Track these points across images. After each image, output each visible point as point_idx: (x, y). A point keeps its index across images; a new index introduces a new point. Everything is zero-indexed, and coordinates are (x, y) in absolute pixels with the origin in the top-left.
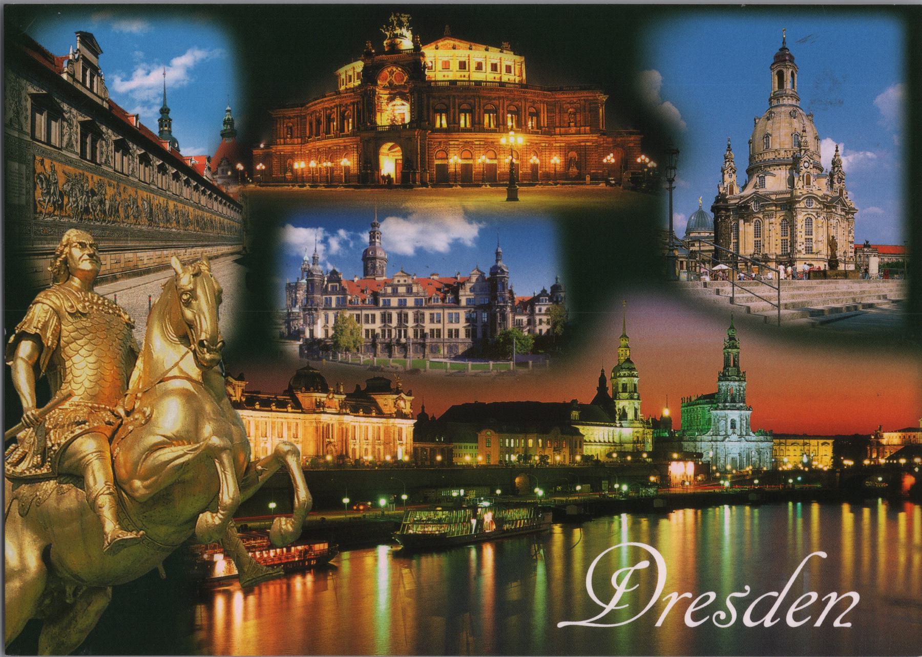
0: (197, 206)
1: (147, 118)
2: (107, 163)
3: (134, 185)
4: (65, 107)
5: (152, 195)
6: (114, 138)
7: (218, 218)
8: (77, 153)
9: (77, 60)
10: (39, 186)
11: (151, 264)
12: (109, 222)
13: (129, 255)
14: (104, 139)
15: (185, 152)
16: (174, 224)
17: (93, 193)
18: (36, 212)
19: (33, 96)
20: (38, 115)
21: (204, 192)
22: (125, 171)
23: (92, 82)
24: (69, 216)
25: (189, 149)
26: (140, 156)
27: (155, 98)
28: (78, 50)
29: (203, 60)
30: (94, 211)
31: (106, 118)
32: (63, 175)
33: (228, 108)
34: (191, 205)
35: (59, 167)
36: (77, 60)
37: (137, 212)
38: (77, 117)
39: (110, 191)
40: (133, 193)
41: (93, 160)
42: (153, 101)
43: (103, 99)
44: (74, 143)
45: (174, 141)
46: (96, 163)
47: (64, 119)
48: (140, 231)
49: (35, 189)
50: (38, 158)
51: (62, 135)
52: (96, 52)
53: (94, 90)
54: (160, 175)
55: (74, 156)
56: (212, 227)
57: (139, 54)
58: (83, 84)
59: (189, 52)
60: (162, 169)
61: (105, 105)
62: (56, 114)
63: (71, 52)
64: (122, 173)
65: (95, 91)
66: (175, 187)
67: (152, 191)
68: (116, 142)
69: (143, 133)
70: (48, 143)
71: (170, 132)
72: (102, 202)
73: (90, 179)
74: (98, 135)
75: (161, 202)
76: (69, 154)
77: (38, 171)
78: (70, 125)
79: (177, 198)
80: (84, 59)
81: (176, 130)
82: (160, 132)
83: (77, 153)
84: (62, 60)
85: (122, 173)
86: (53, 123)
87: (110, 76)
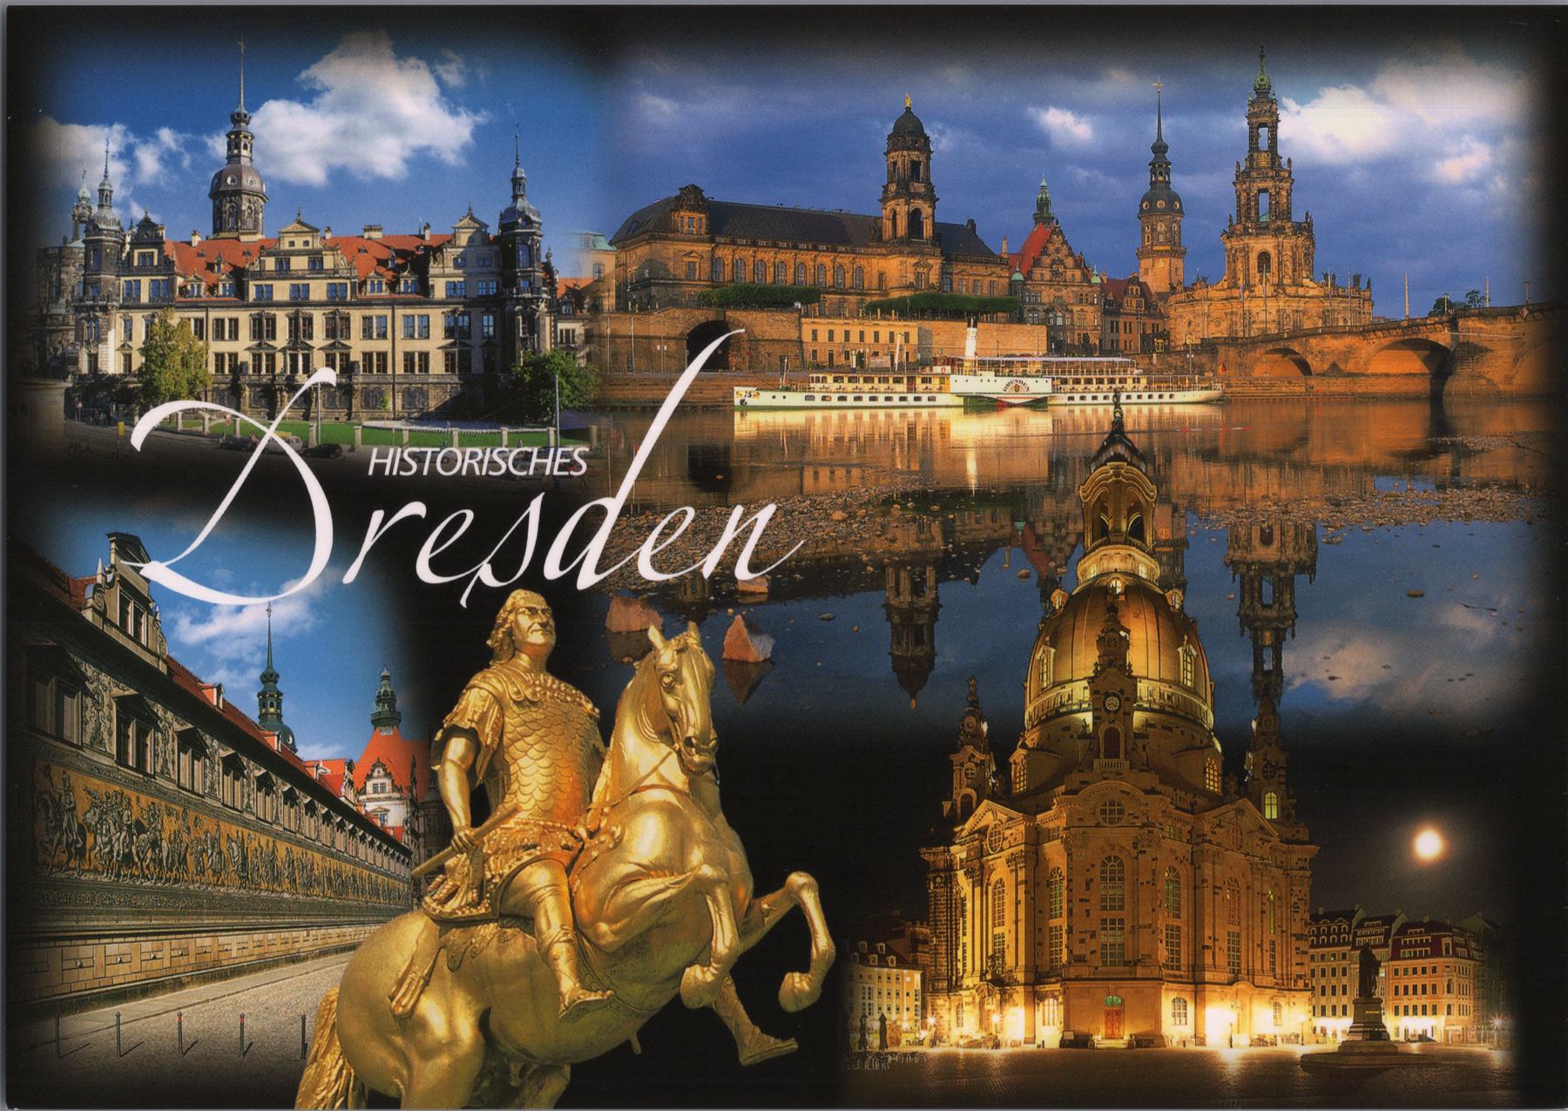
0: (328, 852)
1: (236, 689)
3: (213, 812)
4: (90, 670)
5: (246, 832)
6: (178, 727)
7: (366, 872)
8: (110, 756)
9: (111, 585)
11: (248, 958)
12: (168, 880)
13: (205, 941)
14: (158, 729)
15: (309, 752)
16: (286, 884)
17: (141, 829)
21: (341, 826)
22: (198, 788)
24: (96, 871)
25: (311, 749)
26: (225, 760)
27: (252, 654)
28: (113, 566)
30: (142, 860)
34: (318, 850)
36: (111, 585)
37: (220, 861)
39: (170, 825)
40: (212, 827)
41: (140, 766)
42: (248, 659)
43: (158, 657)
44: (106, 736)
45: (286, 733)
47: (87, 693)
48: (227, 896)
53: (143, 643)
55: (106, 761)
58: (122, 628)
60: (264, 784)
61: (163, 668)
63: (100, 570)
64: (192, 792)
65: (143, 641)
66: (288, 816)
67: (246, 824)
68: (181, 735)
71: (279, 716)
72: (155, 844)
73: (134, 803)
74: (149, 724)
75: (263, 843)
76: (96, 757)
78: (97, 703)
79: (291, 837)
81: (290, 712)
82: (263, 716)
83: (110, 756)
86: (67, 699)
87: (170, 615)
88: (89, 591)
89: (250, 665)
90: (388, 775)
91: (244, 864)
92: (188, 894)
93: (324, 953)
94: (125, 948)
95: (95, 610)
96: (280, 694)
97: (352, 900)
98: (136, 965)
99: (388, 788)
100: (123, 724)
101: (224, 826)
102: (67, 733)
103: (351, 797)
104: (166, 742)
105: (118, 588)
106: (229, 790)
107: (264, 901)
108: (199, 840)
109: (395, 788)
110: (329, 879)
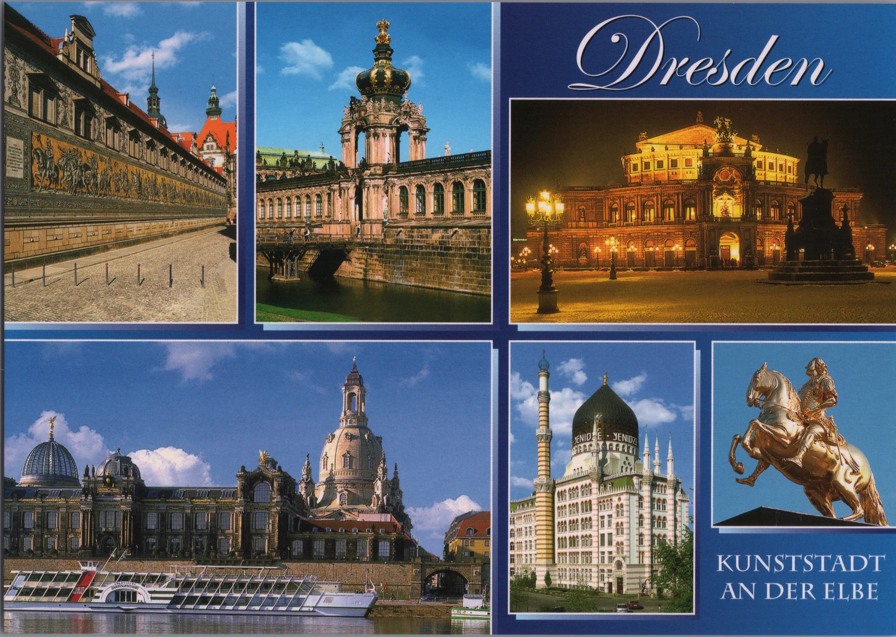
0: (184, 180)
1: (139, 98)
2: (99, 139)
4: (61, 86)
5: (141, 170)
6: (106, 116)
8: (71, 130)
9: (72, 42)
10: (35, 162)
11: (141, 235)
12: (100, 195)
13: (120, 226)
14: (96, 117)
17: (87, 168)
18: (32, 185)
19: (30, 76)
20: (35, 94)
21: (190, 167)
23: (85, 62)
24: (64, 190)
25: (175, 127)
26: (130, 133)
27: (144, 78)
28: (73, 32)
29: (190, 42)
30: (87, 185)
31: (98, 97)
32: (57, 150)
33: (213, 88)
34: (178, 180)
35: (54, 143)
36: (72, 42)
38: (72, 96)
39: (102, 166)
40: (124, 169)
41: (87, 136)
42: (142, 80)
44: (69, 120)
45: (161, 119)
46: (90, 140)
47: (59, 98)
48: (131, 203)
49: (32, 163)
50: (35, 134)
51: (58, 113)
52: (90, 35)
54: (149, 151)
56: (198, 200)
57: (129, 37)
58: (78, 64)
59: (176, 35)
60: (151, 145)
61: (98, 85)
62: (52, 93)
64: (113, 149)
66: (163, 162)
67: (141, 166)
68: (107, 120)
69: (134, 111)
70: (45, 120)
71: (158, 110)
72: (94, 176)
73: (83, 154)
74: (91, 115)
76: (63, 131)
77: (35, 147)
78: (64, 103)
79: (164, 172)
80: (79, 41)
82: (149, 110)
83: (71, 130)
84: (59, 41)
85: (113, 149)
86: (49, 101)
87: (102, 58)
88: (61, 46)
89: (143, 84)
90: (214, 141)
91: (140, 186)
92: (112, 202)
93: (182, 232)
94: (79, 230)
95: (64, 55)
96: (159, 99)
97: (197, 205)
98: (84, 239)
99: (215, 147)
100: (78, 114)
101: (130, 167)
102: (49, 118)
103: (195, 151)
104: (100, 124)
105: (76, 44)
106: (133, 148)
107: (150, 205)
108: (117, 174)
109: (218, 147)
110: (184, 194)
